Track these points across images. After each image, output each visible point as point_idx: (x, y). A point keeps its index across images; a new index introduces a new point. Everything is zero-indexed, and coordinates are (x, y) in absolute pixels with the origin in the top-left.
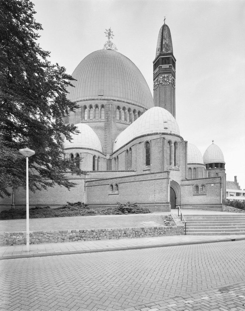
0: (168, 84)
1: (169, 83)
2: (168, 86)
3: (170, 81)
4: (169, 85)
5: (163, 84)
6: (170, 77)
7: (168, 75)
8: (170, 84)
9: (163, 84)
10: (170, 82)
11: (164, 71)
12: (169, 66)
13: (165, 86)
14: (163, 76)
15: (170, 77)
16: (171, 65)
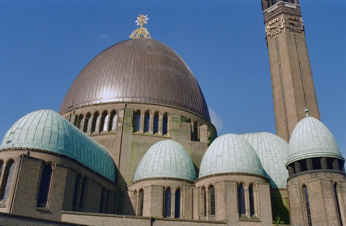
0: (280, 30)
1: (281, 29)
2: (281, 33)
3: (283, 25)
4: (281, 32)
5: (271, 36)
6: (282, 19)
7: (278, 18)
8: (282, 30)
9: (271, 36)
10: (282, 27)
11: (270, 16)
12: (278, 4)
13: (275, 37)
14: (270, 23)
15: (280, 20)
16: (280, 2)
